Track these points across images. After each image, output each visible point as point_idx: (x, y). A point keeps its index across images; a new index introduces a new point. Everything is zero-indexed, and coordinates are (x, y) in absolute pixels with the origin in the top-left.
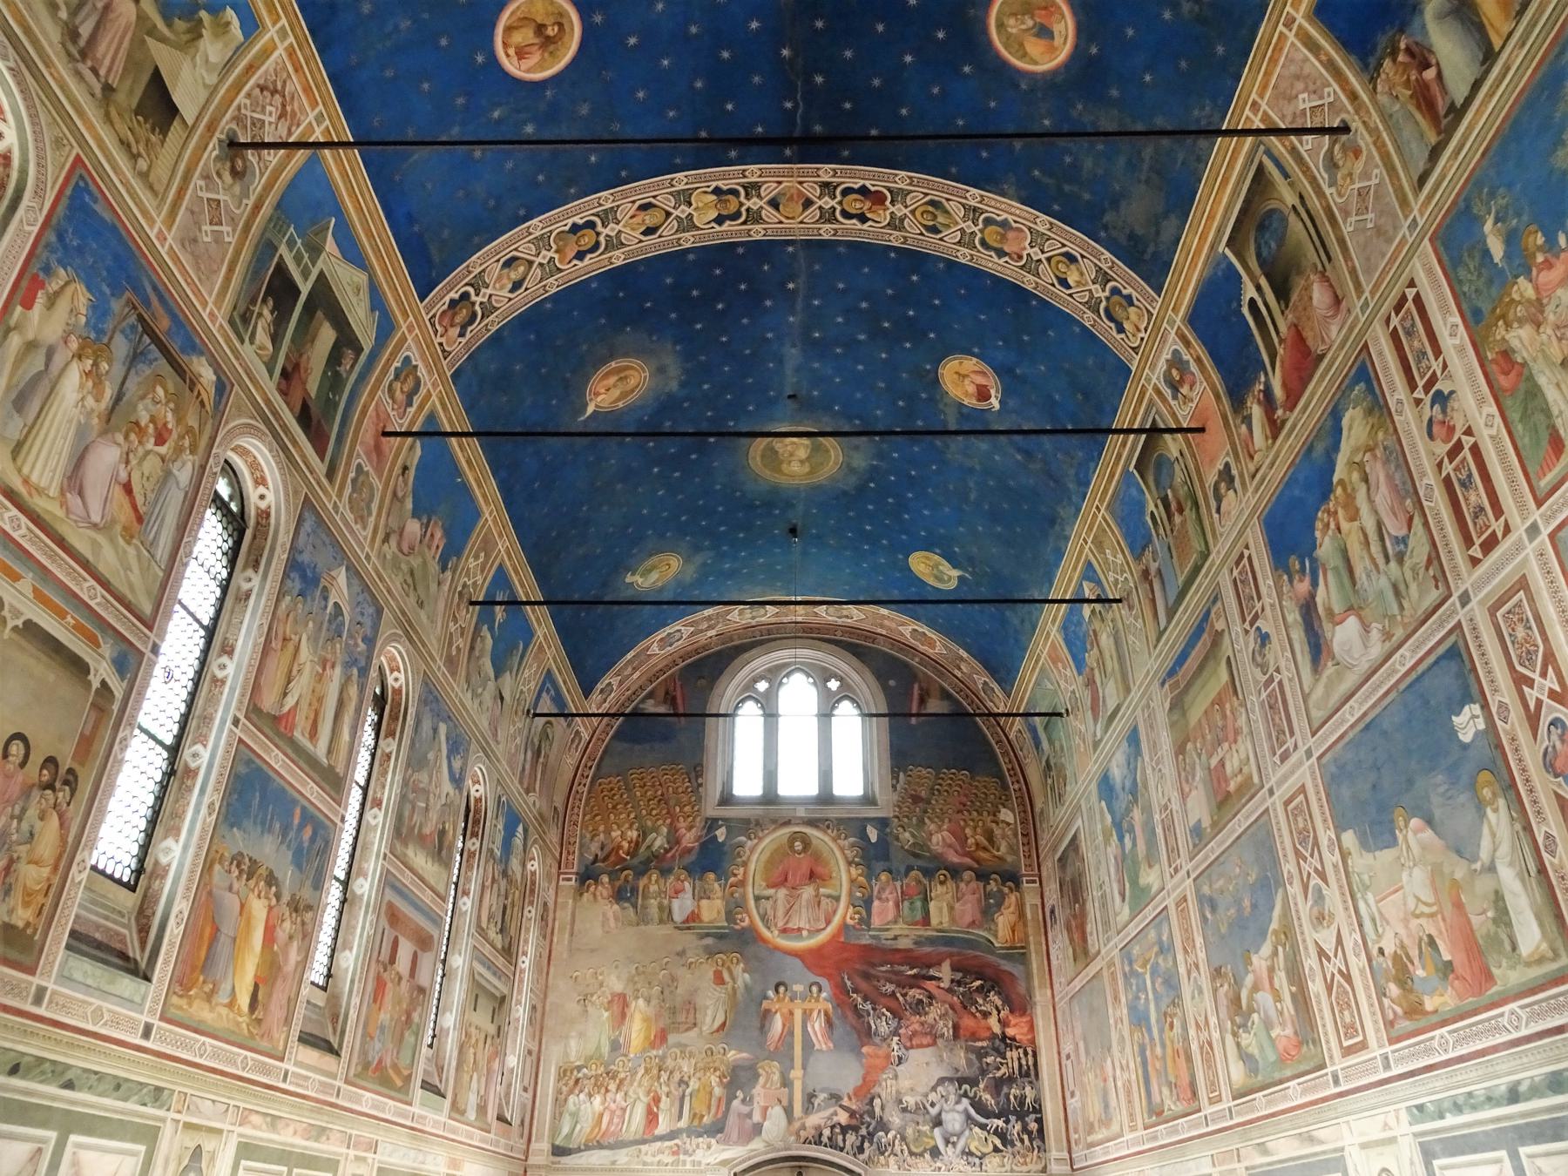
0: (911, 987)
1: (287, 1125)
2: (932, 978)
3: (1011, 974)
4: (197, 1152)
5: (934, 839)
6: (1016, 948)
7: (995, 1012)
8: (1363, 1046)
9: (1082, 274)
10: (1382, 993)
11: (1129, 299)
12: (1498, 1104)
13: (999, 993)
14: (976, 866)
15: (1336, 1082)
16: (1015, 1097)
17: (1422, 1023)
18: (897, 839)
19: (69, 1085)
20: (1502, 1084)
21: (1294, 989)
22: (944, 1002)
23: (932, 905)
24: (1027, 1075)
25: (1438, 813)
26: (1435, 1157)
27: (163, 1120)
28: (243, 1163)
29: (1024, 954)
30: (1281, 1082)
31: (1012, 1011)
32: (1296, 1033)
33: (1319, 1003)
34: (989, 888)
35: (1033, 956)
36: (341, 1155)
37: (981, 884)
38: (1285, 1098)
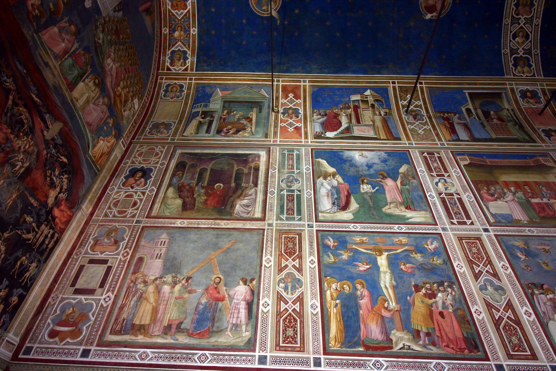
0: (25, 106)
2: (45, 122)
3: (84, 177)
5: (109, 61)
6: (96, 166)
7: (58, 189)
9: (523, 43)
11: (530, 66)
13: (69, 180)
14: (113, 102)
16: (21, 265)
18: (97, 28)
22: (36, 145)
23: (81, 85)
24: (42, 254)
29: (96, 173)
31: (67, 200)
34: (109, 120)
35: (99, 180)
37: (108, 114)
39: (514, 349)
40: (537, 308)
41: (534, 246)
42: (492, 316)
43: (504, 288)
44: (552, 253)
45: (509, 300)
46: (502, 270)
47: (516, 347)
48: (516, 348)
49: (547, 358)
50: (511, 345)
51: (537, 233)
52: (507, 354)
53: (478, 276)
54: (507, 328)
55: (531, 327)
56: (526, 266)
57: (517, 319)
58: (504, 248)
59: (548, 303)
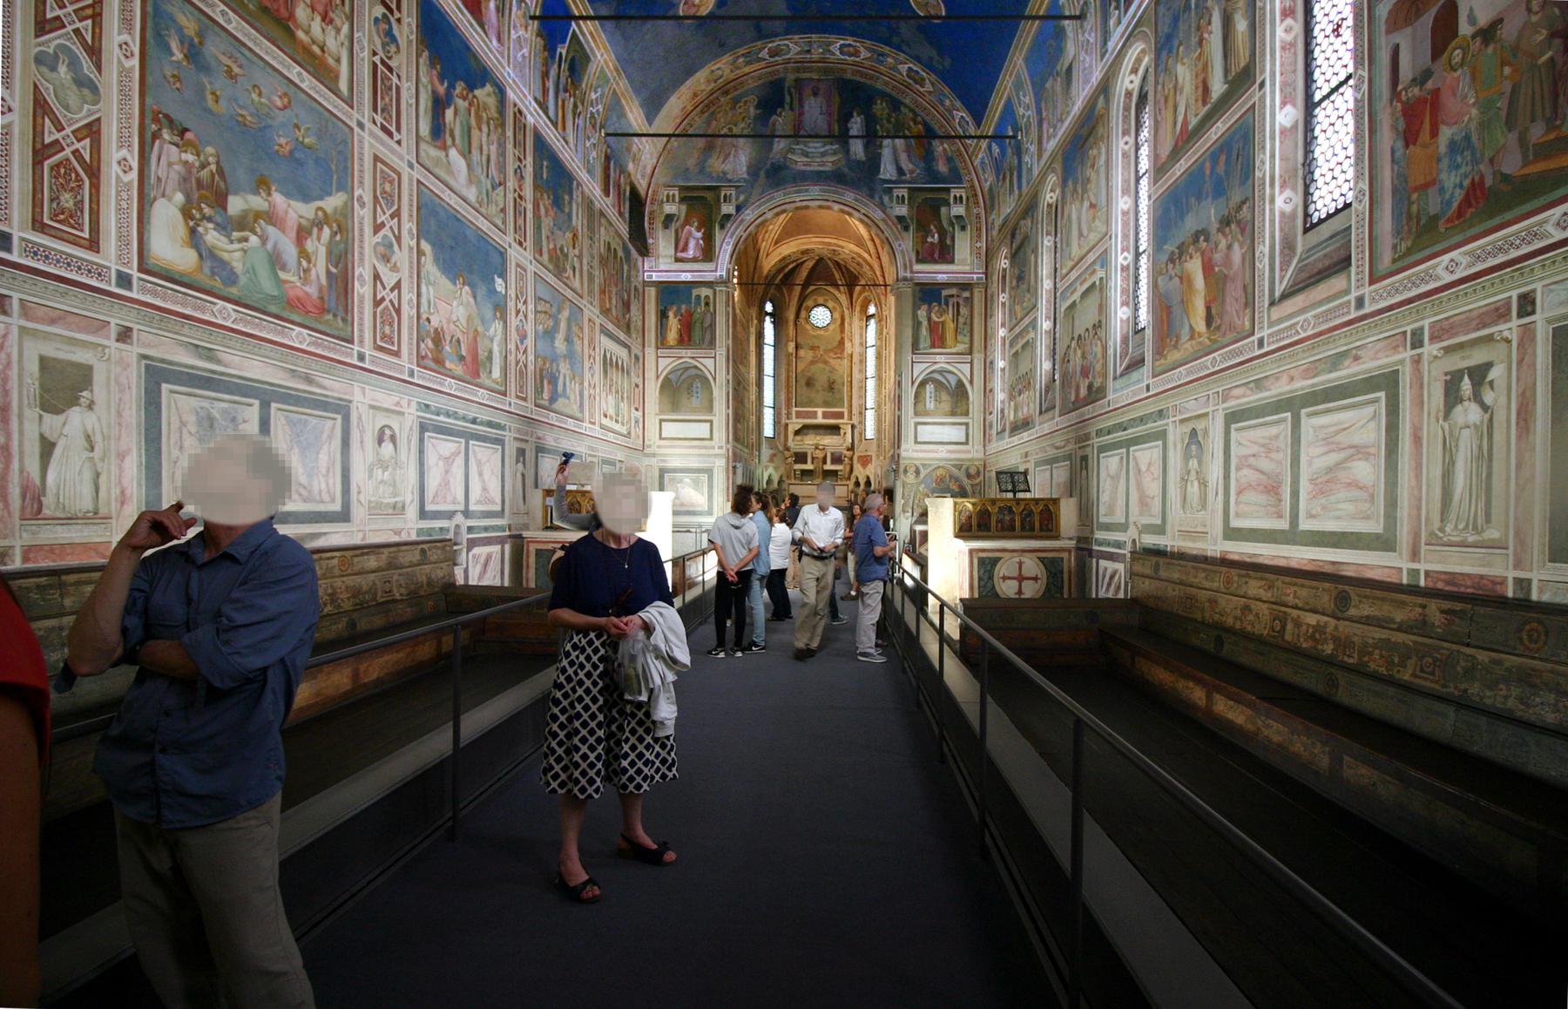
1: (1278, 379)
4: (1194, 433)
8: (397, 354)
10: (420, 339)
12: (467, 421)
15: (361, 357)
17: (442, 370)
19: (1125, 429)
20: (471, 415)
21: (334, 270)
25: (479, 298)
26: (428, 431)
27: (1167, 424)
28: (1233, 426)
30: (293, 323)
32: (322, 298)
33: (362, 302)
36: (1402, 362)
38: (282, 333)
39: (56, 215)
40: (149, 167)
41: (214, 49)
42: (38, 132)
43: (102, 90)
44: (239, 85)
45: (98, 120)
46: (117, 50)
47: (63, 213)
48: (62, 217)
49: (119, 257)
50: (55, 205)
51: (235, 28)
52: (34, 220)
53: (48, 27)
54: (62, 171)
55: (118, 193)
56: (174, 76)
57: (95, 164)
58: (150, 9)
59: (176, 167)
